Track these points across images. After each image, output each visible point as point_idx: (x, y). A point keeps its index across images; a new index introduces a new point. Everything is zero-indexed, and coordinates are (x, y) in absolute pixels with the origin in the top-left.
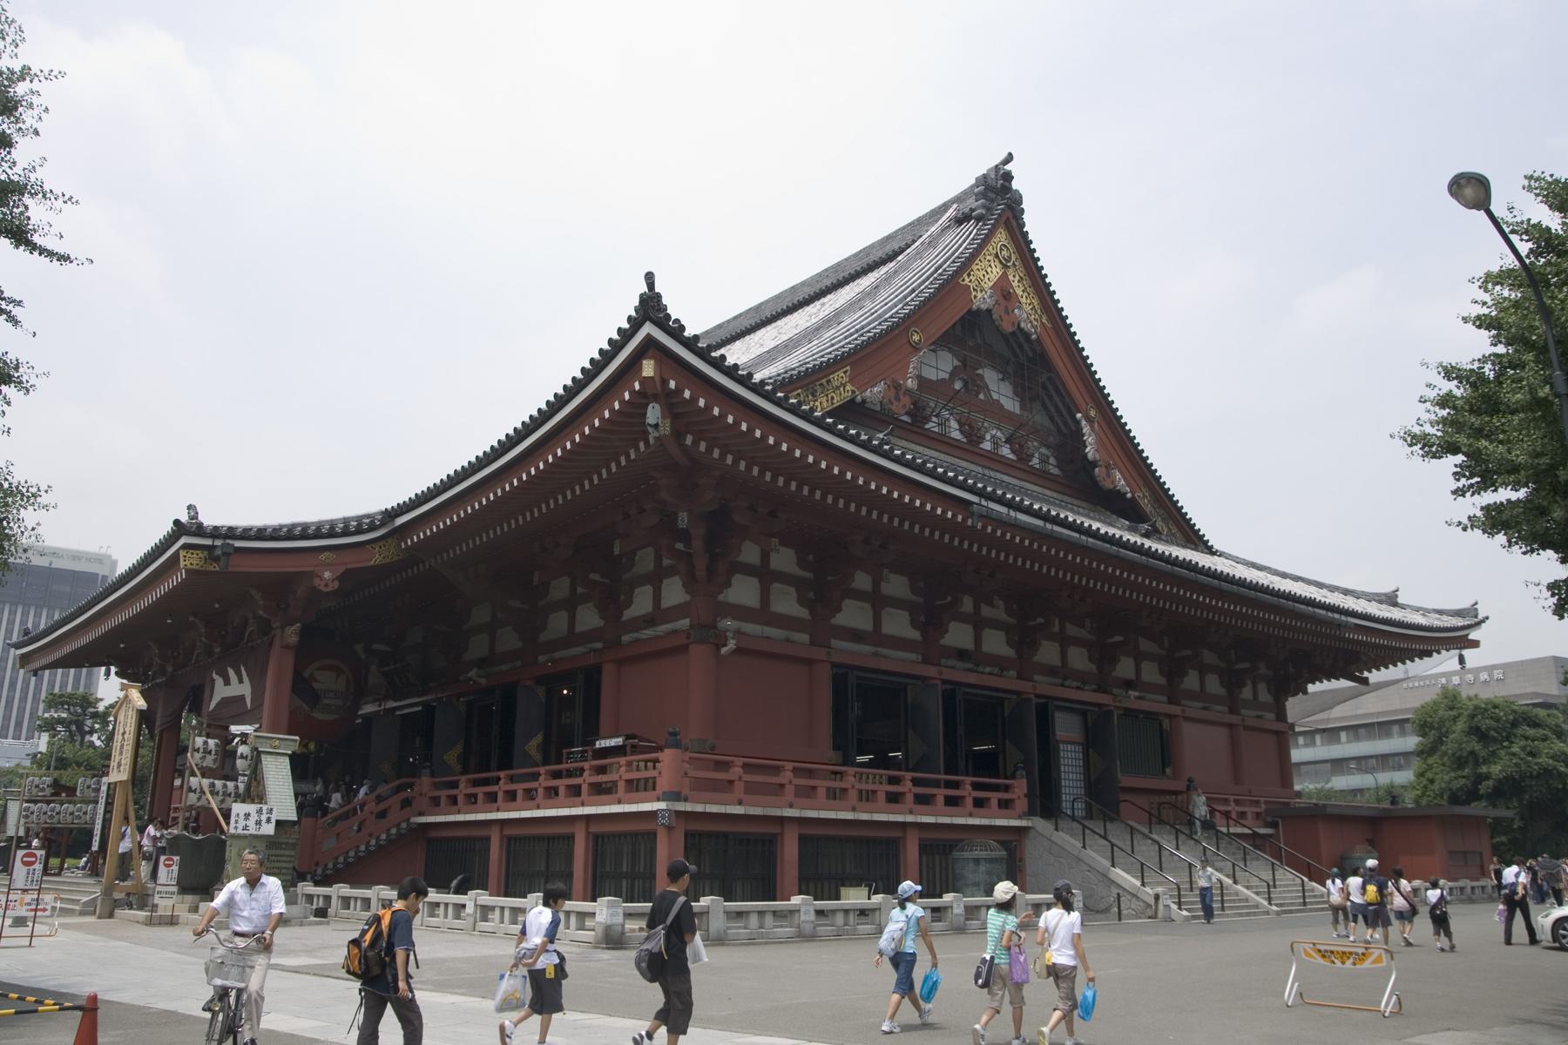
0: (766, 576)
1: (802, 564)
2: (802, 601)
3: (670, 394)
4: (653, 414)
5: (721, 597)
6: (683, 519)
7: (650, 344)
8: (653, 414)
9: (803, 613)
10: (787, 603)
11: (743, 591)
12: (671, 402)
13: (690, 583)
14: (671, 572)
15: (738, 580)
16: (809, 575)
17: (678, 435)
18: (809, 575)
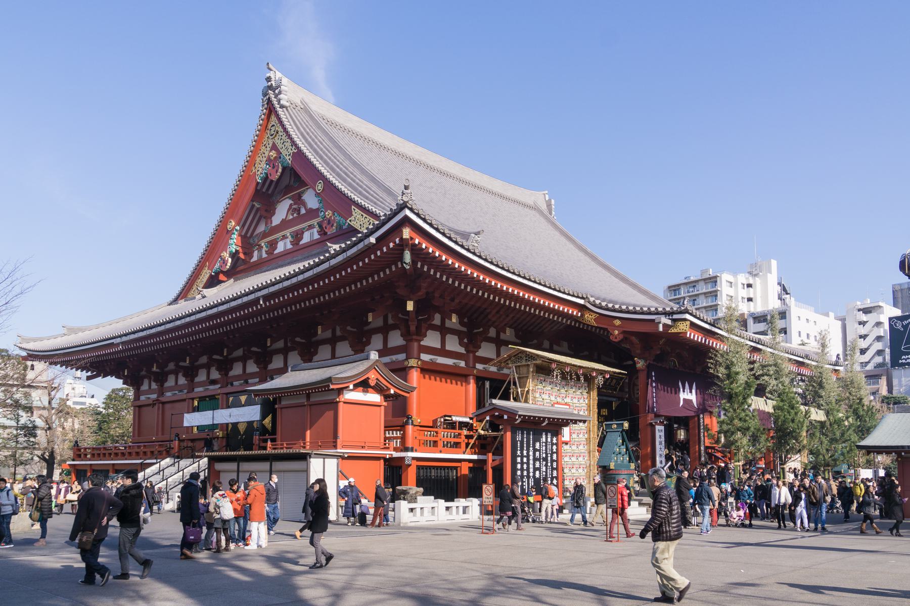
0: (444, 331)
1: (461, 323)
2: (461, 344)
3: (414, 245)
4: (407, 257)
5: (422, 343)
6: (410, 306)
7: (407, 221)
8: (407, 257)
9: (462, 350)
10: (453, 344)
11: (432, 340)
12: (417, 251)
13: (406, 335)
14: (394, 327)
15: (429, 333)
16: (465, 329)
17: (414, 262)
18: (465, 329)
